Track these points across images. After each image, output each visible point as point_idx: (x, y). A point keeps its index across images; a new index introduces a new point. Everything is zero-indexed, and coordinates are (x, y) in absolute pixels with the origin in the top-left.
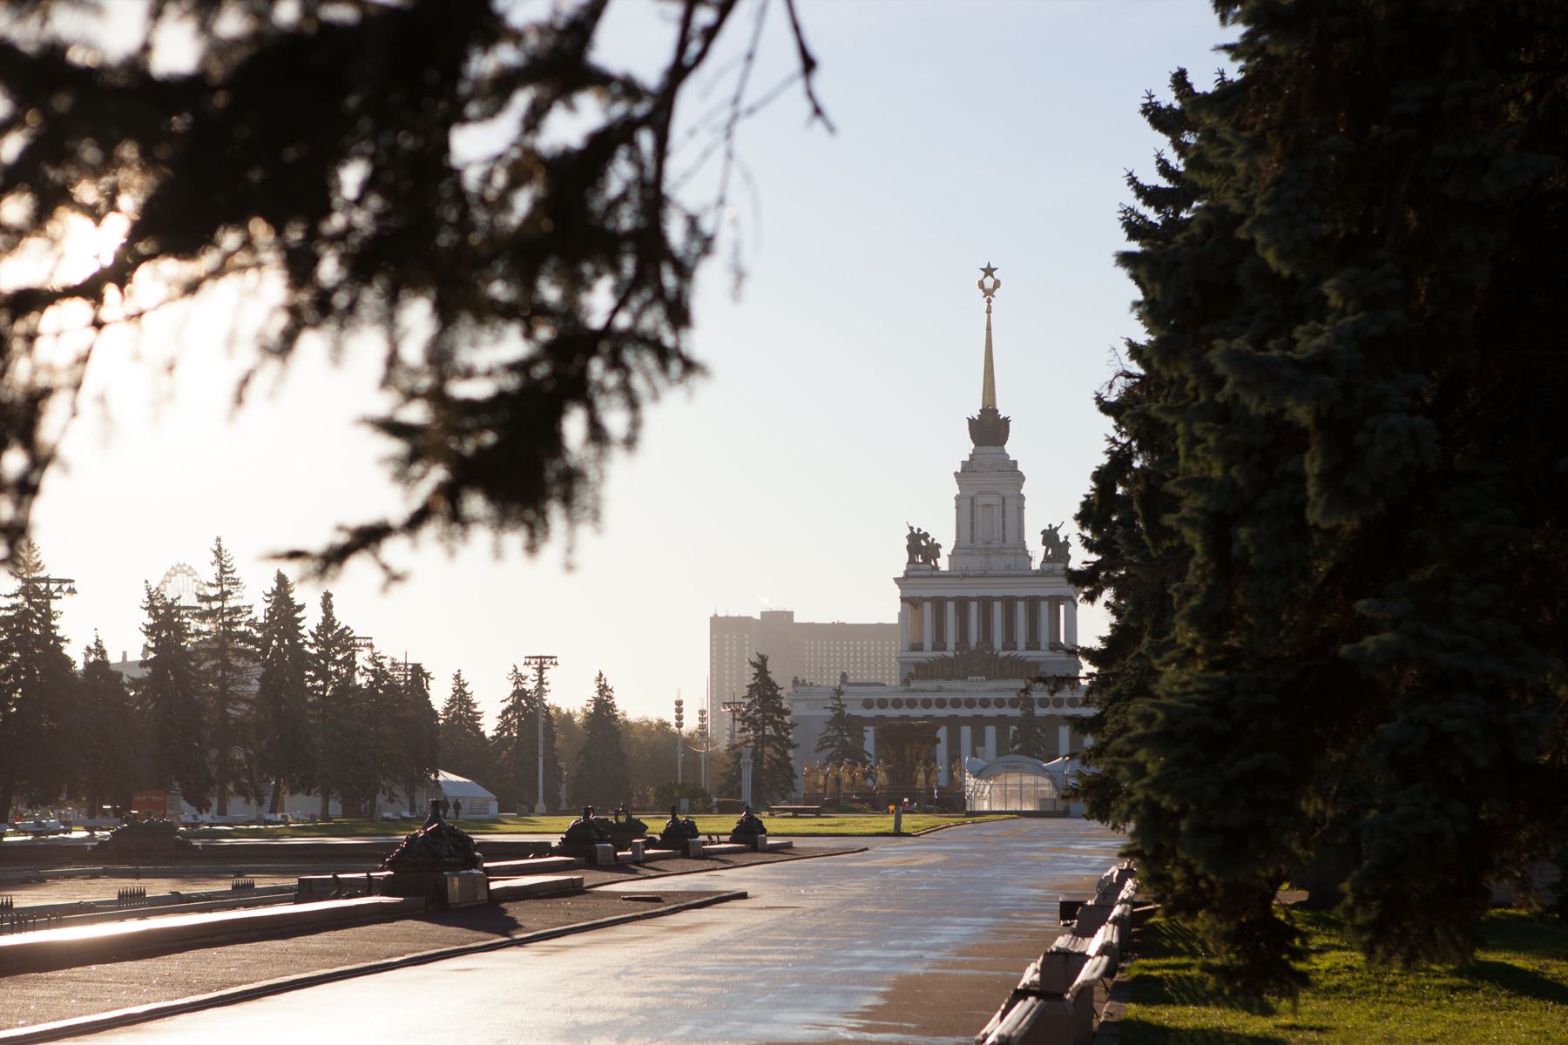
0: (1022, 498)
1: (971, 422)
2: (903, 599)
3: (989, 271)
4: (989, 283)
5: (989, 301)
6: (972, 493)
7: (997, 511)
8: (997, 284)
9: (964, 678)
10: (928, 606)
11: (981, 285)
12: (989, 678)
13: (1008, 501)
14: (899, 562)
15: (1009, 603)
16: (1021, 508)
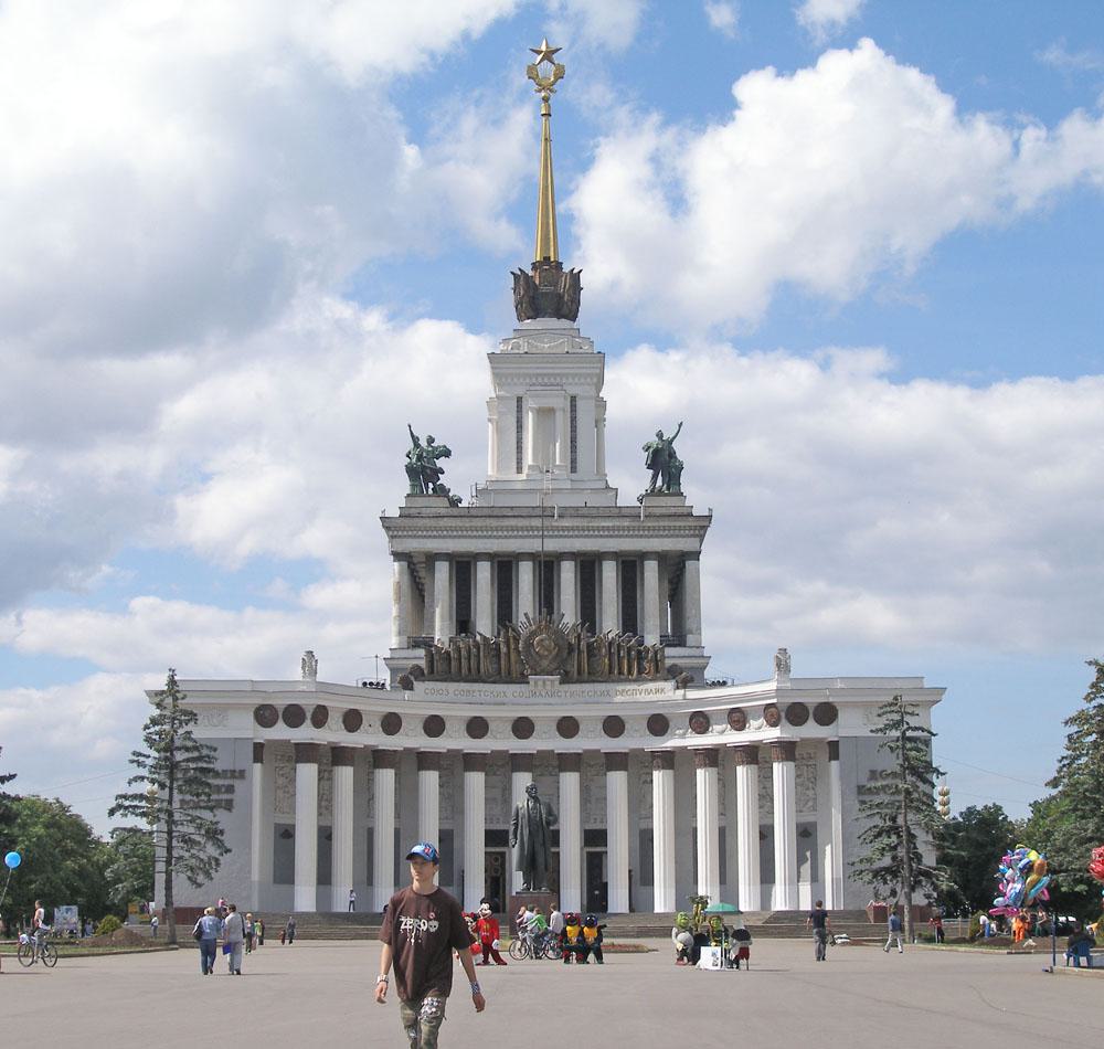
0: (601, 405)
1: (520, 278)
2: (397, 556)
3: (548, 56)
4: (547, 70)
5: (546, 100)
6: (520, 391)
7: (562, 422)
8: (560, 75)
9: (523, 680)
10: (442, 571)
11: (532, 72)
12: (566, 679)
13: (579, 403)
14: (395, 493)
15: (588, 566)
16: (599, 422)
